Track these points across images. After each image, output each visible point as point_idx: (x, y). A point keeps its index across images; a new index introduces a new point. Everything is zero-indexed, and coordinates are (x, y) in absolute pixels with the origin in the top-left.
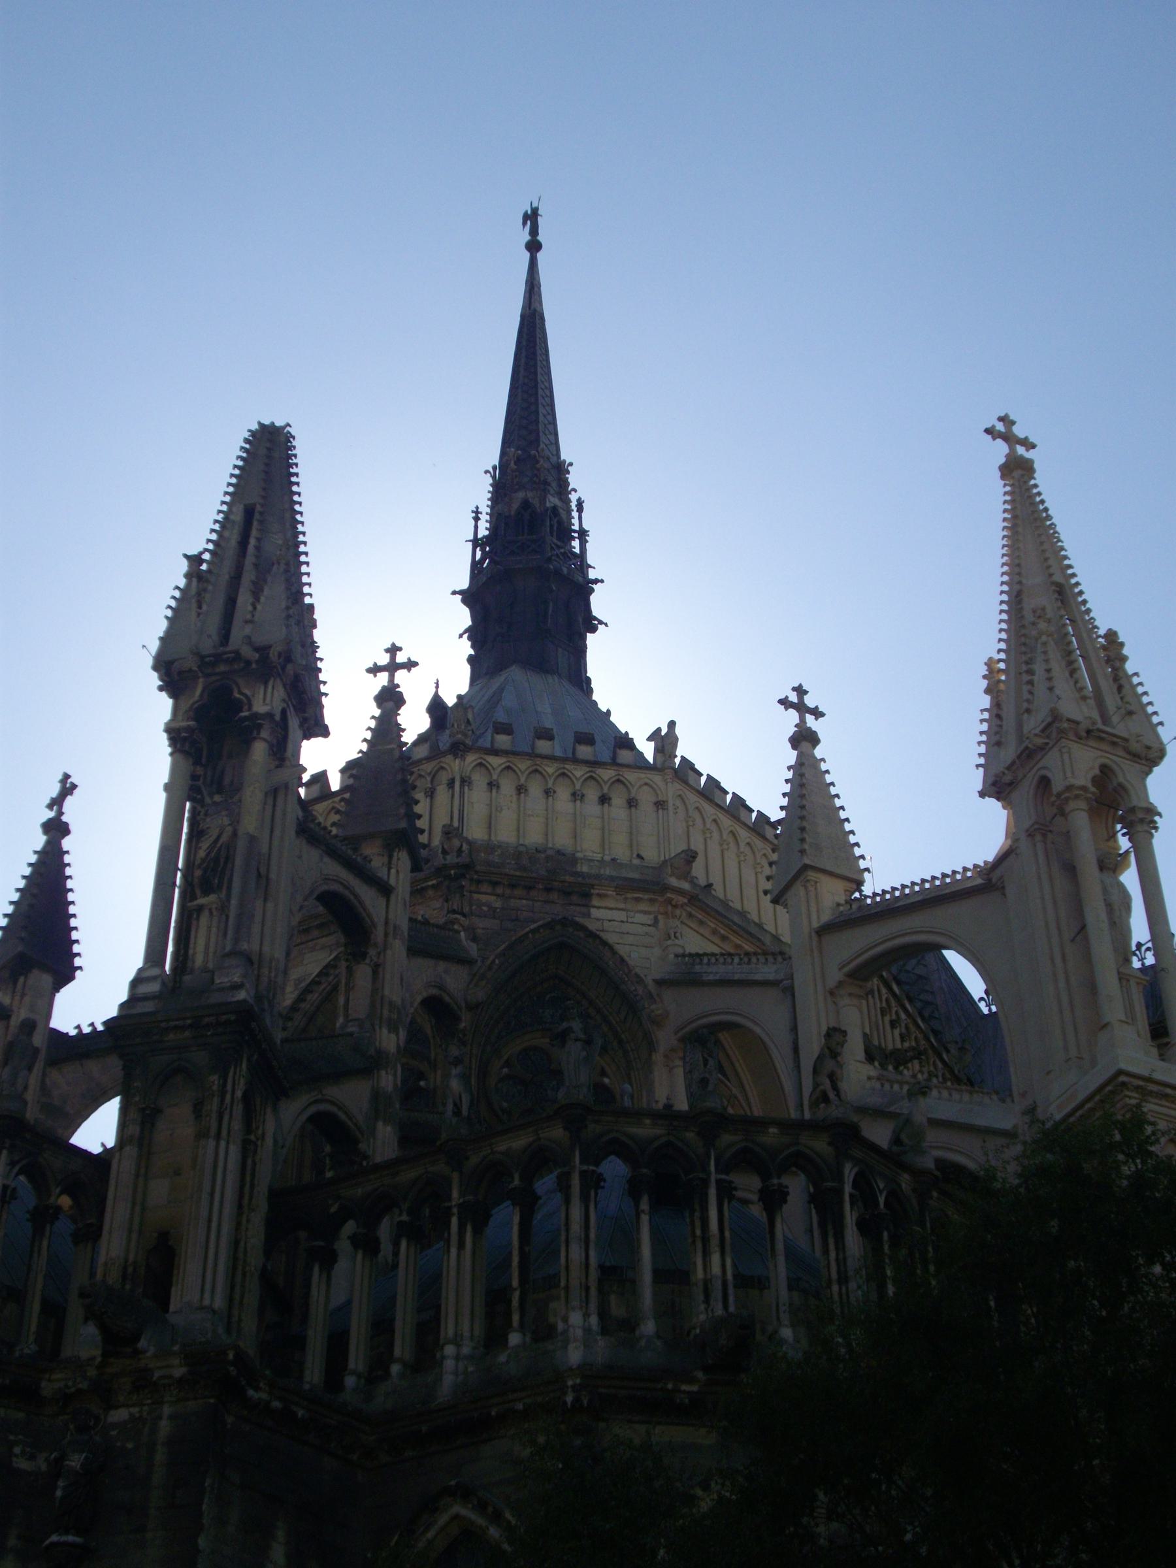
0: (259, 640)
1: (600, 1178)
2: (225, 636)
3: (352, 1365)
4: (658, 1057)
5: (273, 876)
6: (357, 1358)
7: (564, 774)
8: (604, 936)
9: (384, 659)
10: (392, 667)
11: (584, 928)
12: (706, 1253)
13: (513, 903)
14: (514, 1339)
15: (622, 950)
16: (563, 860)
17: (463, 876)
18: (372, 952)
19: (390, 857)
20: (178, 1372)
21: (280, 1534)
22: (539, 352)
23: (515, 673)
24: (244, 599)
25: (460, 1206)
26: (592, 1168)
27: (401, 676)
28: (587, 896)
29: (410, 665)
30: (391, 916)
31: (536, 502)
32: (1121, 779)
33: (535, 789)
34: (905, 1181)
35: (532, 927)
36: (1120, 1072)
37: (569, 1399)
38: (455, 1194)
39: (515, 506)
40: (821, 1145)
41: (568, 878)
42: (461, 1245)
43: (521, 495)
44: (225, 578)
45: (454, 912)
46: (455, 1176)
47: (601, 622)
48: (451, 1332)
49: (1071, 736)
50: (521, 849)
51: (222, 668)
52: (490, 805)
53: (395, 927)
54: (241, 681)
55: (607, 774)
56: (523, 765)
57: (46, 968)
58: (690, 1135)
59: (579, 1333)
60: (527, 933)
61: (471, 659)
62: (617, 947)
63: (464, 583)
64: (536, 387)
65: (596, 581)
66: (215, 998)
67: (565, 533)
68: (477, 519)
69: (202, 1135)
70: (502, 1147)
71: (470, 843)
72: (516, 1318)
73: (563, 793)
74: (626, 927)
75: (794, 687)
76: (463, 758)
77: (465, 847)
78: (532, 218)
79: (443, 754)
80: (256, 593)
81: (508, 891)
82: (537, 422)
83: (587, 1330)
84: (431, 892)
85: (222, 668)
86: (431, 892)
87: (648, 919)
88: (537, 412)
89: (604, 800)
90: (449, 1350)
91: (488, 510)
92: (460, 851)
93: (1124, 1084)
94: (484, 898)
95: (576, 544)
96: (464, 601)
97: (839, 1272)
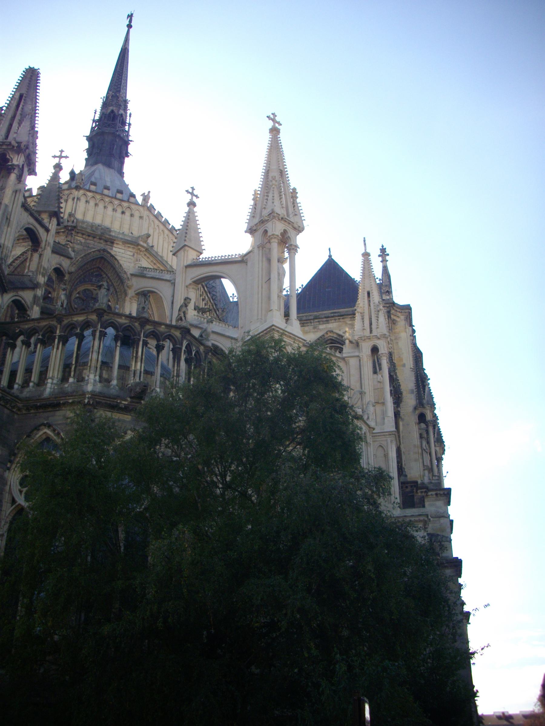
0: (19, 140)
1: (106, 333)
2: (7, 137)
3: (17, 381)
4: (127, 299)
5: (11, 219)
6: (19, 379)
7: (111, 202)
8: (116, 257)
9: (58, 154)
10: (61, 157)
11: (110, 253)
12: (136, 362)
13: (88, 241)
14: (71, 380)
15: (121, 262)
17: (73, 230)
18: (40, 250)
19: (50, 220)
22: (125, 62)
23: (100, 166)
24: (15, 125)
25: (59, 336)
26: (104, 330)
27: (63, 161)
28: (113, 243)
29: (66, 157)
30: (48, 239)
31: (116, 111)
32: (289, 235)
33: (101, 205)
34: (202, 348)
35: (94, 250)
36: (273, 325)
37: (86, 401)
38: (58, 332)
39: (109, 111)
40: (177, 334)
41: (107, 236)
42: (58, 348)
43: (111, 108)
44: (10, 116)
45: (68, 241)
46: (59, 326)
47: (131, 155)
48: (51, 376)
49: (277, 218)
50: (94, 224)
51: (4, 147)
52: (85, 208)
53: (49, 243)
54: (10, 153)
55: (125, 204)
56: (98, 197)
58: (136, 324)
59: (92, 381)
60: (91, 253)
61: (86, 159)
63: (88, 134)
64: (122, 73)
65: (131, 141)
67: (124, 123)
68: (95, 113)
70: (75, 319)
71: (77, 220)
72: (72, 374)
73: (110, 208)
74: (123, 255)
75: (296, 189)
76: (79, 191)
77: (75, 221)
78: (130, 16)
79: (73, 189)
80: (20, 124)
81: (87, 237)
82: (121, 84)
83: (95, 381)
84: (61, 234)
85: (4, 147)
86: (61, 234)
87: (132, 254)
88: (121, 81)
89: (123, 213)
90: (50, 381)
91: (100, 111)
92: (73, 222)
93: (273, 329)
94: (79, 238)
95: (127, 128)
96: (87, 139)
97: (177, 373)
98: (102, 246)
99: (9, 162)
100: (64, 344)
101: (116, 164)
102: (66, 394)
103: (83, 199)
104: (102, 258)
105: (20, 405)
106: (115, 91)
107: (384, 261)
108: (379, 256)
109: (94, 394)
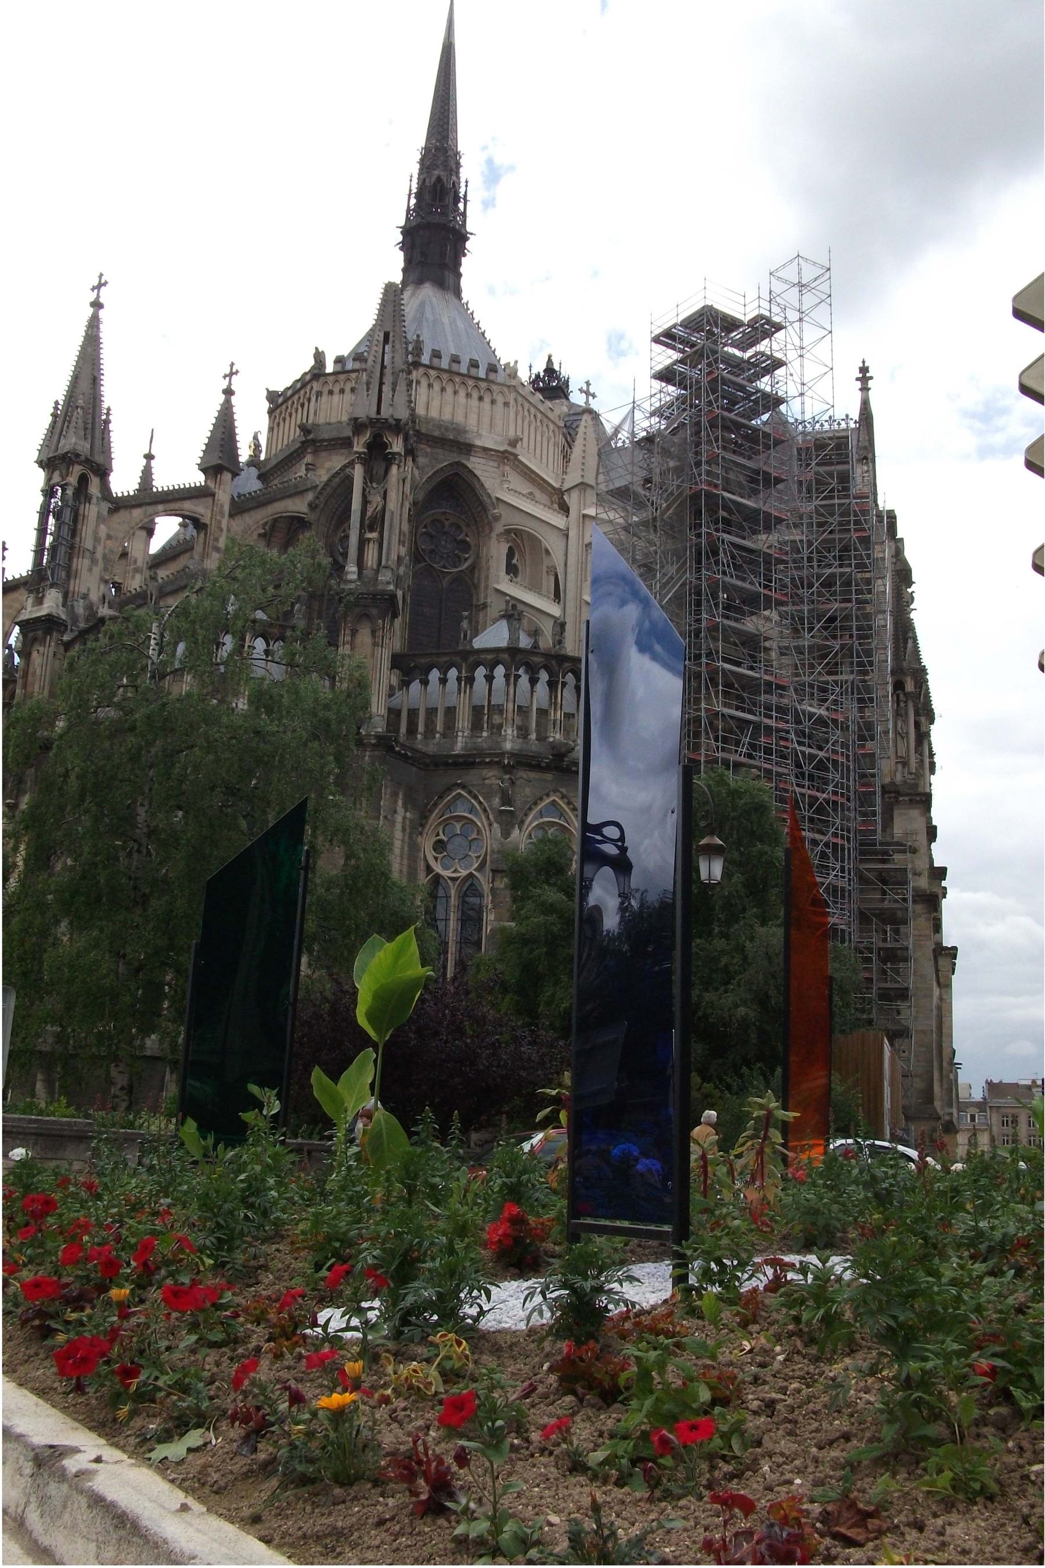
0: (397, 416)
4: (494, 535)
13: (436, 450)
16: (460, 430)
20: (373, 741)
21: (401, 796)
31: (444, 179)
33: (450, 390)
39: (433, 179)
42: (465, 692)
43: (436, 172)
51: (378, 425)
55: (483, 385)
57: (228, 470)
62: (481, 478)
66: (380, 587)
69: (375, 644)
70: (483, 656)
73: (462, 393)
80: (394, 390)
85: (378, 425)
90: (460, 734)
95: (461, 206)
98: (455, 457)
99: (386, 448)
100: (471, 687)
101: (450, 279)
102: (482, 754)
103: (424, 383)
104: (457, 474)
105: (428, 761)
106: (439, 137)
107: (865, 389)
108: (857, 379)
109: (512, 755)
